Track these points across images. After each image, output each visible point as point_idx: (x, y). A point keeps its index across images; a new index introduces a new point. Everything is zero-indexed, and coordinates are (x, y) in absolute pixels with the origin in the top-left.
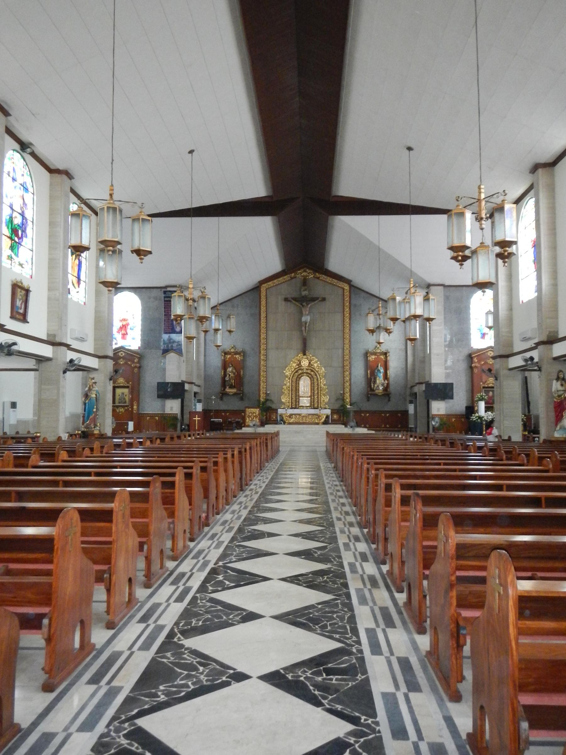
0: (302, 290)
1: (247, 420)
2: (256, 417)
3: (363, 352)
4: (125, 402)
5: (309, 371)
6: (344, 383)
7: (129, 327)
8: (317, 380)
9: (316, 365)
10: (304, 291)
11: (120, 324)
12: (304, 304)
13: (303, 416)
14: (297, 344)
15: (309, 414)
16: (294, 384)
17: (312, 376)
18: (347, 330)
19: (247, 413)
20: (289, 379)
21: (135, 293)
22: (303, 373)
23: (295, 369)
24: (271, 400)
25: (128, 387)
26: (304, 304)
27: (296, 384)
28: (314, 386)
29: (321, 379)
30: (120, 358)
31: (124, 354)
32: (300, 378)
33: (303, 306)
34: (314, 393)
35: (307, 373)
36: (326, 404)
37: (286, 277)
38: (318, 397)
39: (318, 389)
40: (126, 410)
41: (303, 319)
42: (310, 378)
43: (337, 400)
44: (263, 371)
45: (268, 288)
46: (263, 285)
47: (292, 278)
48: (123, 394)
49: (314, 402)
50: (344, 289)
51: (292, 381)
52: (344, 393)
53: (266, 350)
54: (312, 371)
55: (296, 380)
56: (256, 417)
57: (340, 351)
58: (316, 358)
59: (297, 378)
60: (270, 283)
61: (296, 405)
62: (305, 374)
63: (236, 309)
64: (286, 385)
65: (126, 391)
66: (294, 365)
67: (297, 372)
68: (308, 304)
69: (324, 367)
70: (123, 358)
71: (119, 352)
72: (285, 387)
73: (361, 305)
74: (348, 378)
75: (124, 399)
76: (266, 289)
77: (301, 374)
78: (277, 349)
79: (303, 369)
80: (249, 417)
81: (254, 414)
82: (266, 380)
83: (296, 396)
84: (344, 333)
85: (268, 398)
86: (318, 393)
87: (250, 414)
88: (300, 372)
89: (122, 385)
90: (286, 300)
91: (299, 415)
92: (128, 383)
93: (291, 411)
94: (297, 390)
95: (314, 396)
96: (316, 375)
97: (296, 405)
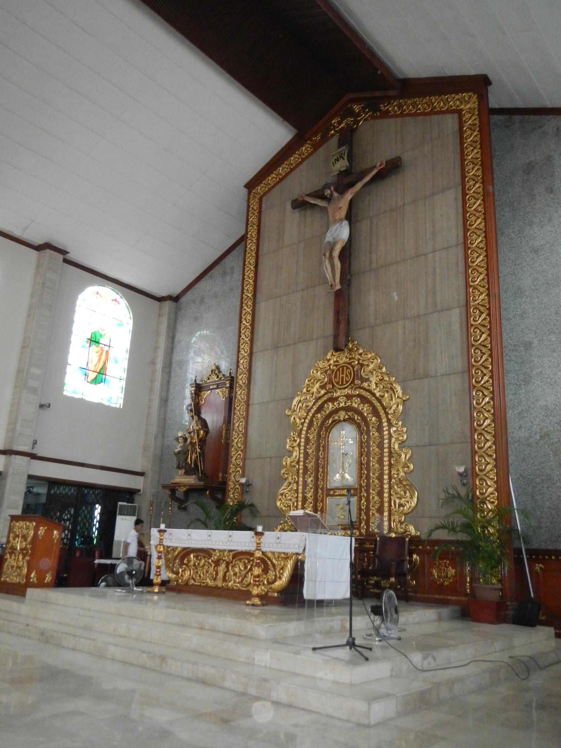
8: (380, 429)
9: (374, 379)
17: (364, 419)
21: (132, 305)
22: (336, 411)
24: (252, 505)
27: (318, 450)
37: (305, 149)
42: (358, 426)
47: (316, 147)
51: (307, 440)
55: (319, 436)
59: (320, 429)
62: (342, 415)
63: (228, 278)
64: (290, 453)
69: (403, 382)
73: (549, 158)
76: (261, 199)
78: (276, 347)
88: (330, 406)
96: (375, 413)
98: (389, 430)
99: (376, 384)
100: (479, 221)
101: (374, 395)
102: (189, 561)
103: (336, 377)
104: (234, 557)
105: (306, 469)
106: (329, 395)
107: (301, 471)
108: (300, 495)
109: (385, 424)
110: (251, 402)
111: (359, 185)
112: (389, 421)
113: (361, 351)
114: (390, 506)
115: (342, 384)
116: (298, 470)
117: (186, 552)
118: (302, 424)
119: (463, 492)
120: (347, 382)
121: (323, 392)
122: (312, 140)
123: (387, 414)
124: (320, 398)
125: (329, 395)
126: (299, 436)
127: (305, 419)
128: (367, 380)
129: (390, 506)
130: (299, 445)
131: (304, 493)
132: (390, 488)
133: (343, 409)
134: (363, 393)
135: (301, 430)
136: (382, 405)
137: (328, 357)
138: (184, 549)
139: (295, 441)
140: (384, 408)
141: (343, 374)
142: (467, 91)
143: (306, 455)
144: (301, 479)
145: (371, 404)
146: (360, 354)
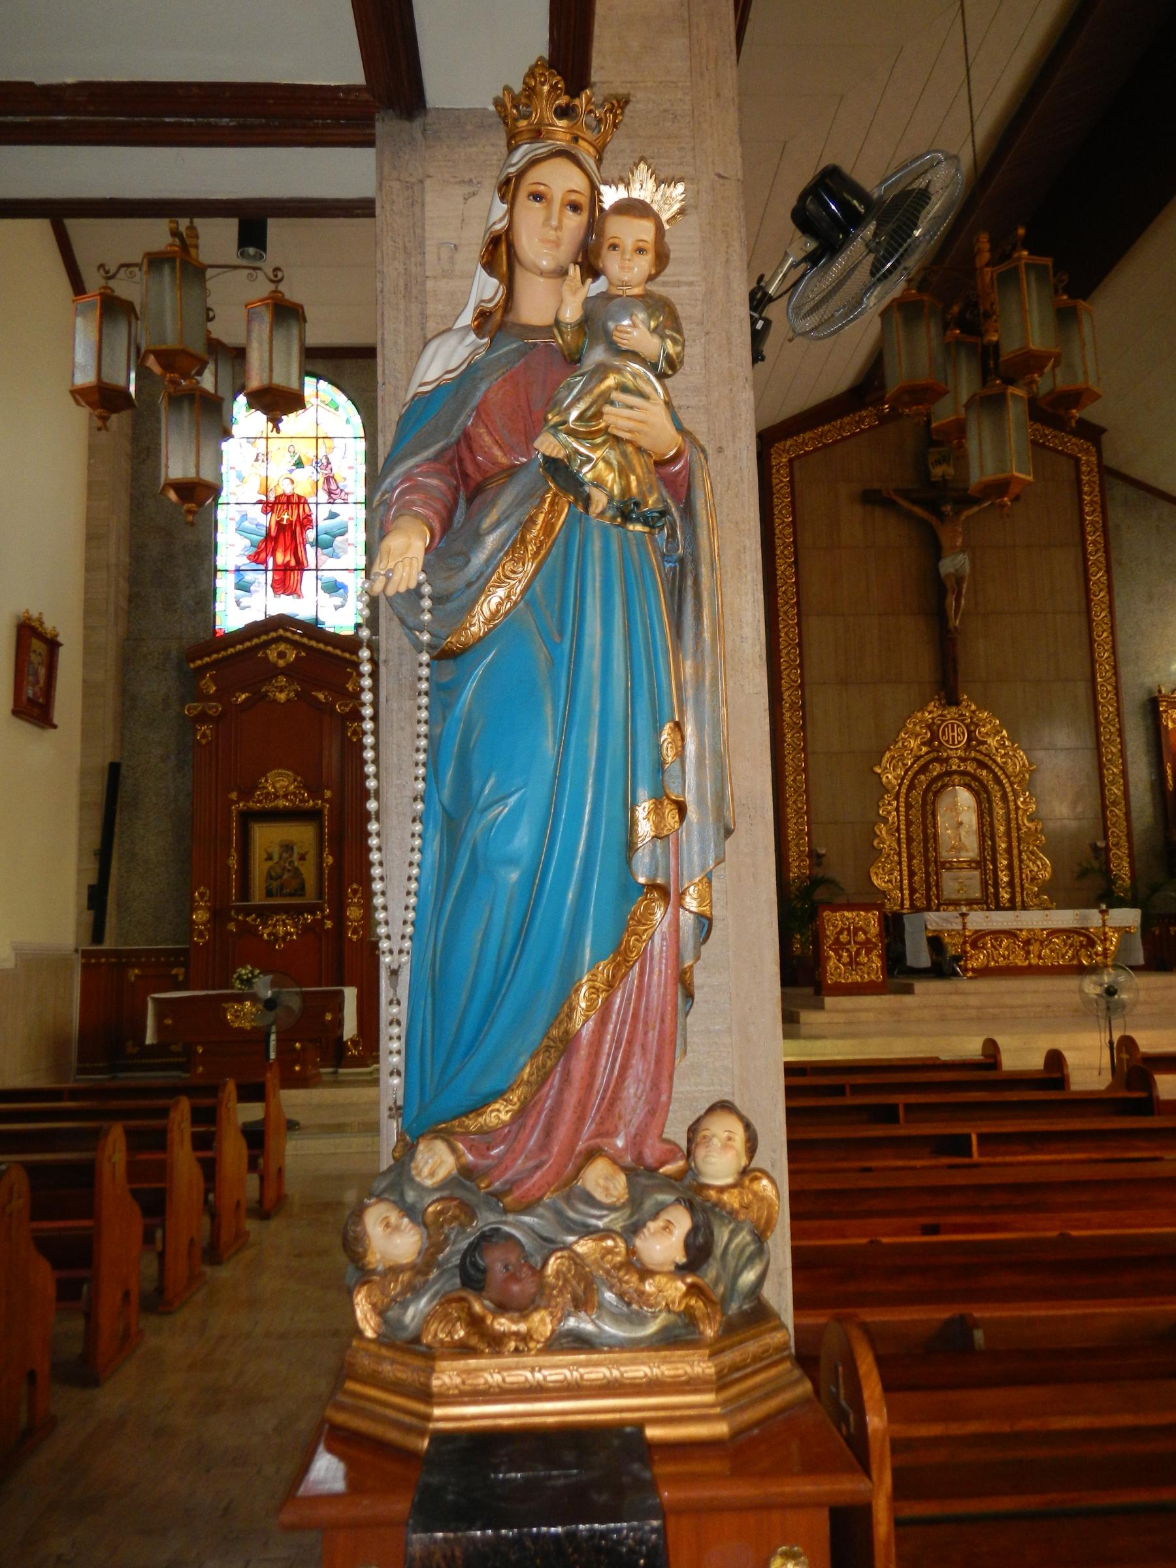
0: (931, 459)
1: (832, 963)
2: (868, 946)
3: (1141, 696)
4: (300, 891)
5: (970, 767)
6: (1104, 808)
7: (311, 534)
8: (1004, 797)
9: (993, 742)
10: (938, 462)
11: (261, 520)
12: (948, 508)
13: (1027, 942)
14: (919, 661)
15: (1054, 932)
16: (915, 814)
18: (1100, 615)
19: (830, 931)
20: (897, 798)
22: (949, 774)
23: (919, 758)
25: (313, 816)
26: (948, 508)
28: (991, 824)
29: (1016, 795)
30: (273, 671)
31: (292, 656)
32: (936, 794)
33: (941, 516)
34: (994, 849)
35: (964, 773)
36: (1045, 888)
38: (1010, 867)
39: (1008, 833)
40: (307, 929)
41: (947, 566)
42: (976, 794)
43: (1084, 873)
44: (797, 771)
45: (798, 457)
46: (780, 445)
48: (288, 847)
49: (996, 885)
50: (1077, 461)
51: (908, 806)
52: (1107, 849)
53: (802, 686)
54: (982, 765)
56: (868, 946)
57: (1082, 688)
58: (995, 716)
60: (807, 440)
61: (928, 899)
62: (956, 778)
64: (885, 820)
65: (302, 834)
66: (913, 744)
67: (924, 769)
68: (958, 513)
70: (290, 671)
71: (266, 645)
72: (882, 830)
74: (1116, 791)
75: (297, 873)
76: (791, 461)
77: (940, 776)
79: (949, 758)
80: (838, 946)
81: (861, 936)
82: (808, 802)
83: (927, 863)
84: (1090, 621)
85: (819, 872)
86: (1009, 850)
87: (844, 937)
88: (937, 769)
89: (282, 803)
90: (870, 498)
91: (1011, 934)
92: (316, 793)
93: (979, 920)
94: (930, 838)
95: (994, 861)
97: (928, 899)
98: (1015, 801)
99: (997, 749)
100: (1102, 594)
101: (995, 761)
102: (985, 944)
103: (944, 734)
104: (1048, 935)
105: (910, 840)
106: (935, 754)
107: (904, 841)
108: (905, 868)
109: (1010, 794)
110: (809, 749)
111: (976, 509)
112: (1013, 790)
113: (973, 707)
114: (1022, 880)
115: (953, 744)
116: (899, 839)
117: (980, 935)
118: (900, 785)
119: (1096, 864)
120: (959, 742)
121: (924, 749)
122: (875, 407)
123: (1012, 784)
124: (922, 756)
125: (935, 754)
126: (897, 798)
127: (903, 779)
128: (985, 743)
129: (1022, 880)
130: (897, 809)
131: (910, 866)
132: (1021, 861)
133: (955, 772)
134: (981, 757)
135: (899, 792)
136: (1005, 773)
137: (929, 709)
138: (976, 932)
139: (889, 804)
140: (1007, 777)
141: (953, 731)
142: (1087, 439)
143: (909, 823)
144: (904, 850)
145: (991, 770)
146: (973, 712)
